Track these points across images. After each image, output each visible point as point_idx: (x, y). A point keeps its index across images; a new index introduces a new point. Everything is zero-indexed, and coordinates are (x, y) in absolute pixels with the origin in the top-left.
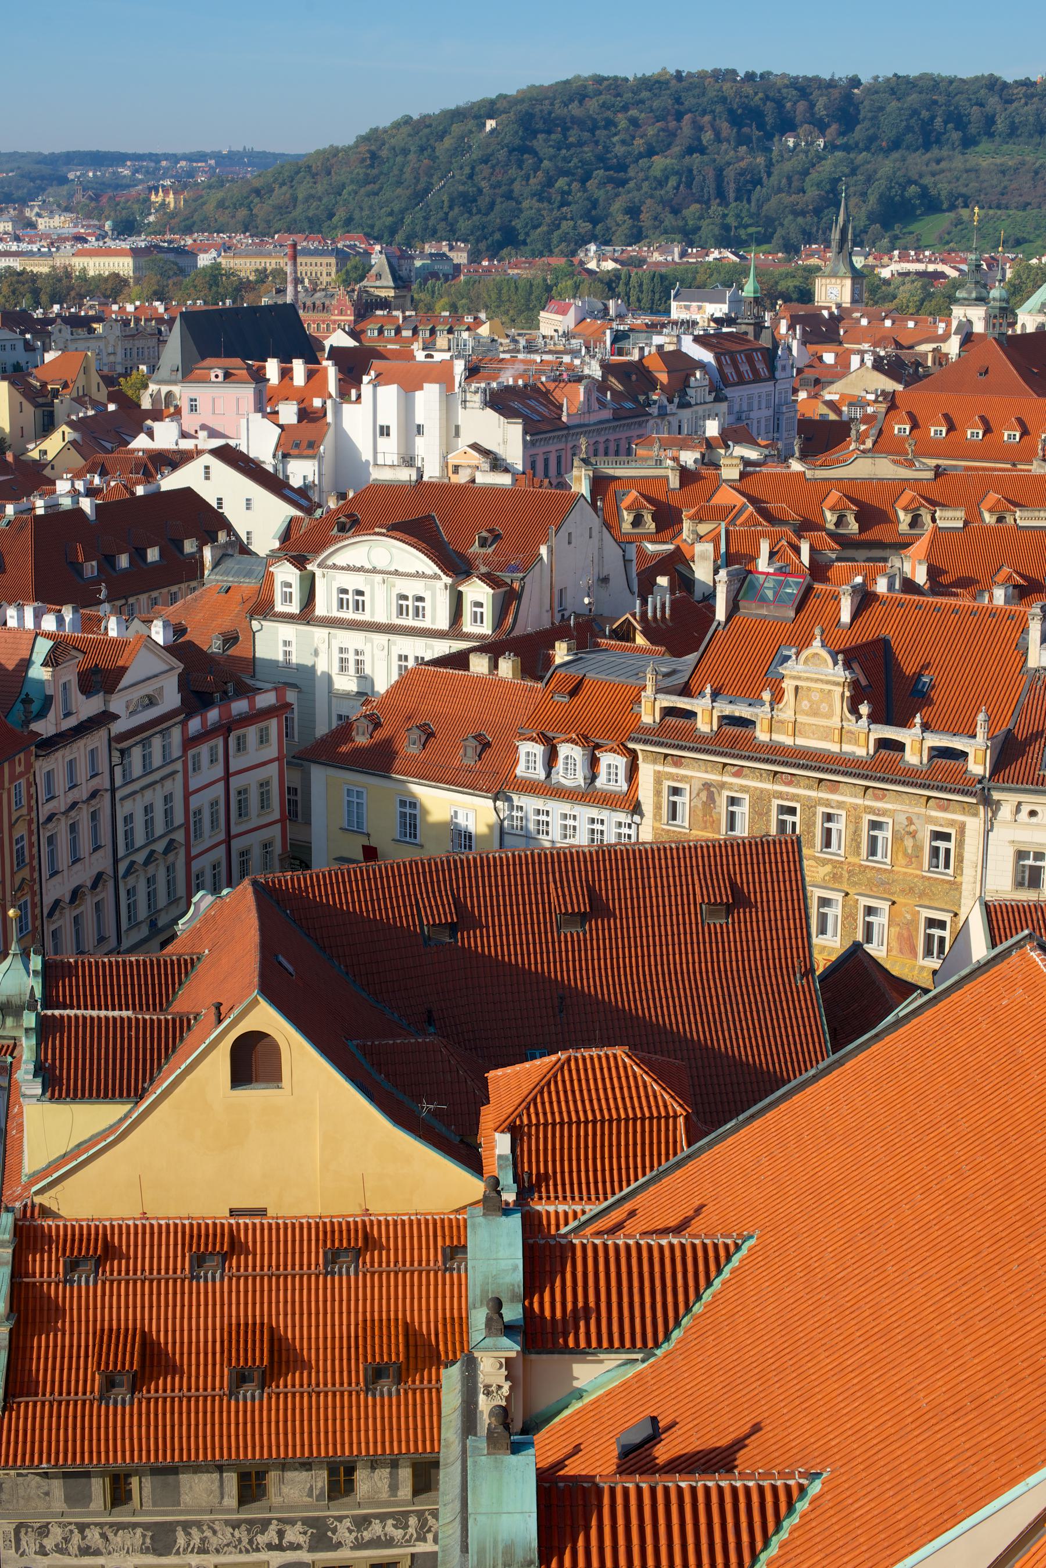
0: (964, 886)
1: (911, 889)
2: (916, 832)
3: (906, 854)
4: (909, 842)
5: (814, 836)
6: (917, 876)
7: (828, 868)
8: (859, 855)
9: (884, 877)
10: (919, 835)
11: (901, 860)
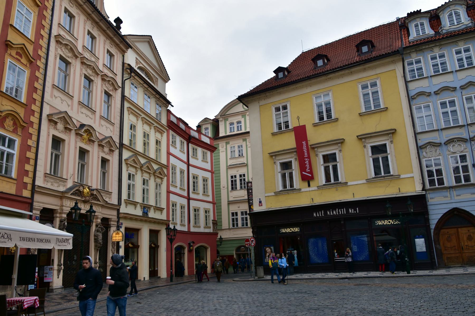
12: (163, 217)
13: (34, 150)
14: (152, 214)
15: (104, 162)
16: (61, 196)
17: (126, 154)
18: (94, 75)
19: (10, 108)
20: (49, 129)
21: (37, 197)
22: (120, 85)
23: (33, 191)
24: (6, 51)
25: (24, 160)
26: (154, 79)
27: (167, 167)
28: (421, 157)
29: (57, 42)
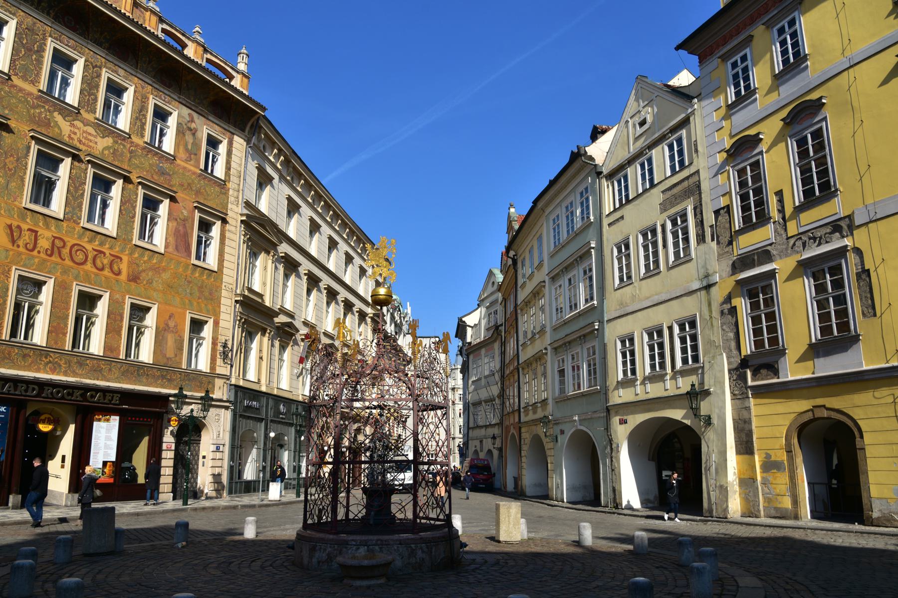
0: (231, 192)
1: (189, 184)
2: (196, 130)
3: (187, 150)
4: (189, 138)
5: (96, 100)
6: (194, 173)
7: (109, 141)
8: (143, 136)
9: (166, 165)
10: (199, 134)
11: (182, 155)
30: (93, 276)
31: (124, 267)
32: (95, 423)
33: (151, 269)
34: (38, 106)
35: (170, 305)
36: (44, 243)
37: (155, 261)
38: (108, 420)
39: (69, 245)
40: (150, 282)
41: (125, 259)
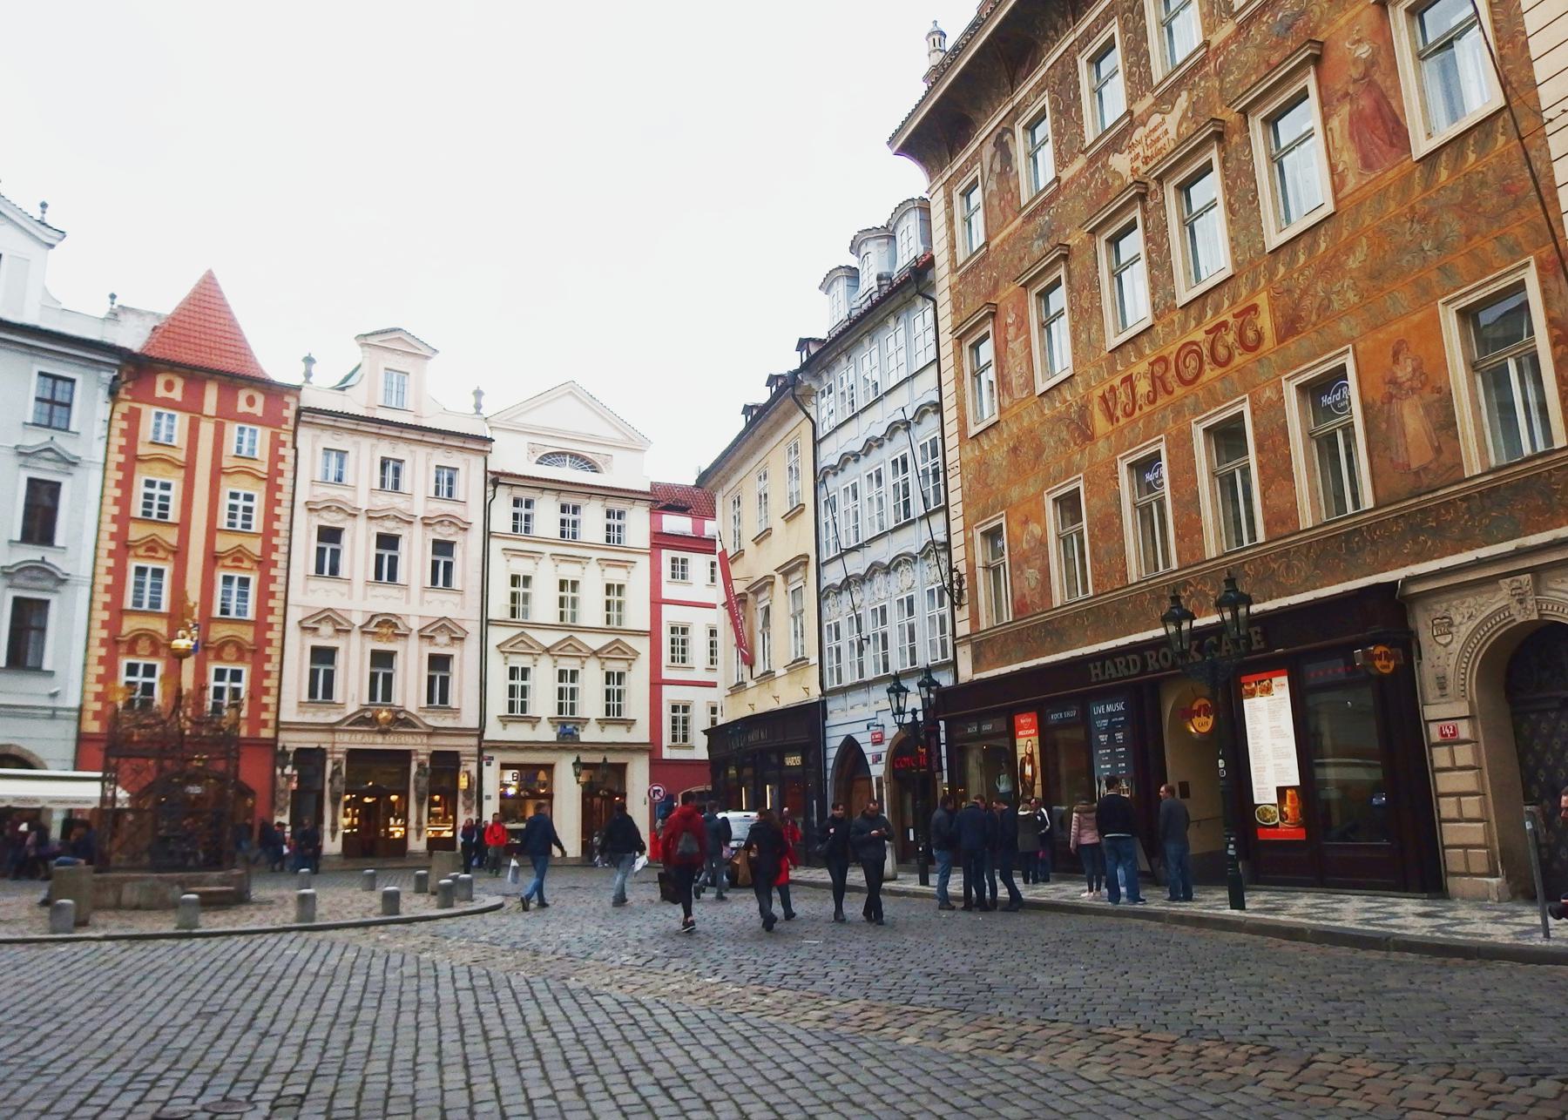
12: (641, 734)
13: (275, 675)
14: (589, 735)
15: (439, 663)
16: (331, 728)
17: (497, 636)
18: (401, 525)
19: (229, 633)
20: (302, 641)
21: (283, 736)
22: (477, 519)
23: (278, 729)
24: (215, 563)
25: (257, 690)
26: (599, 461)
27: (654, 635)
28: (824, 618)
29: (310, 510)
30: (1218, 385)
31: (1265, 322)
32: (1246, 702)
33: (1320, 273)
34: (1093, 175)
35: (1387, 322)
36: (1143, 387)
37: (1323, 246)
38: (1268, 690)
39: (1172, 358)
40: (1324, 307)
41: (1262, 300)
